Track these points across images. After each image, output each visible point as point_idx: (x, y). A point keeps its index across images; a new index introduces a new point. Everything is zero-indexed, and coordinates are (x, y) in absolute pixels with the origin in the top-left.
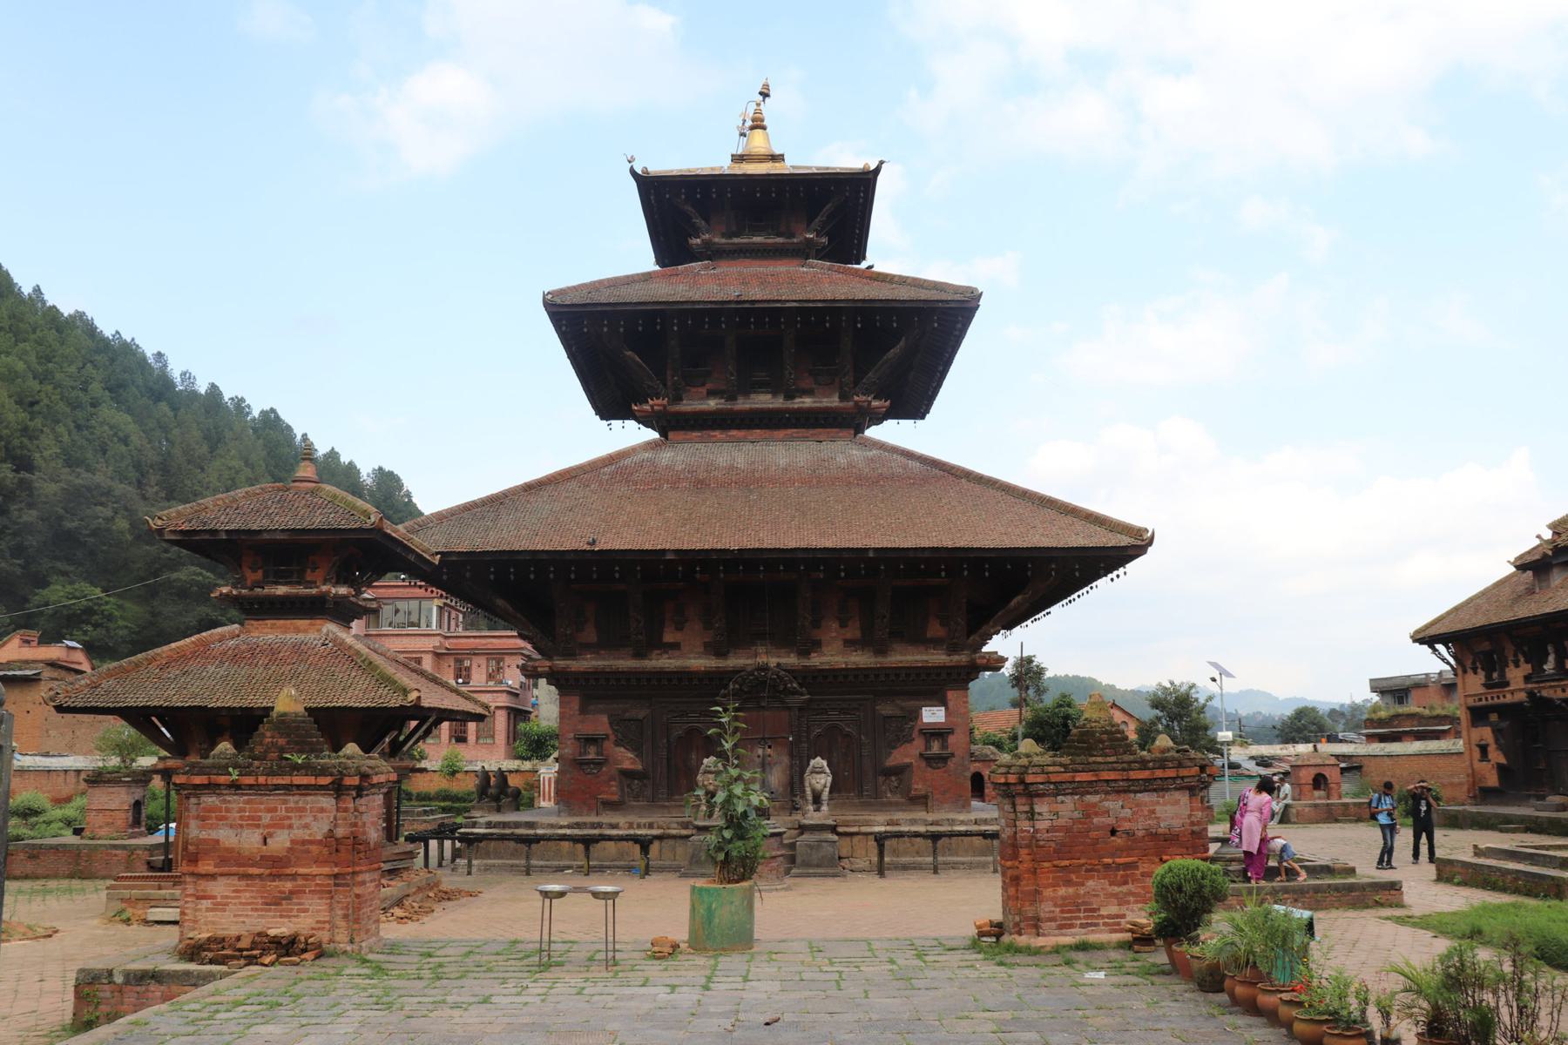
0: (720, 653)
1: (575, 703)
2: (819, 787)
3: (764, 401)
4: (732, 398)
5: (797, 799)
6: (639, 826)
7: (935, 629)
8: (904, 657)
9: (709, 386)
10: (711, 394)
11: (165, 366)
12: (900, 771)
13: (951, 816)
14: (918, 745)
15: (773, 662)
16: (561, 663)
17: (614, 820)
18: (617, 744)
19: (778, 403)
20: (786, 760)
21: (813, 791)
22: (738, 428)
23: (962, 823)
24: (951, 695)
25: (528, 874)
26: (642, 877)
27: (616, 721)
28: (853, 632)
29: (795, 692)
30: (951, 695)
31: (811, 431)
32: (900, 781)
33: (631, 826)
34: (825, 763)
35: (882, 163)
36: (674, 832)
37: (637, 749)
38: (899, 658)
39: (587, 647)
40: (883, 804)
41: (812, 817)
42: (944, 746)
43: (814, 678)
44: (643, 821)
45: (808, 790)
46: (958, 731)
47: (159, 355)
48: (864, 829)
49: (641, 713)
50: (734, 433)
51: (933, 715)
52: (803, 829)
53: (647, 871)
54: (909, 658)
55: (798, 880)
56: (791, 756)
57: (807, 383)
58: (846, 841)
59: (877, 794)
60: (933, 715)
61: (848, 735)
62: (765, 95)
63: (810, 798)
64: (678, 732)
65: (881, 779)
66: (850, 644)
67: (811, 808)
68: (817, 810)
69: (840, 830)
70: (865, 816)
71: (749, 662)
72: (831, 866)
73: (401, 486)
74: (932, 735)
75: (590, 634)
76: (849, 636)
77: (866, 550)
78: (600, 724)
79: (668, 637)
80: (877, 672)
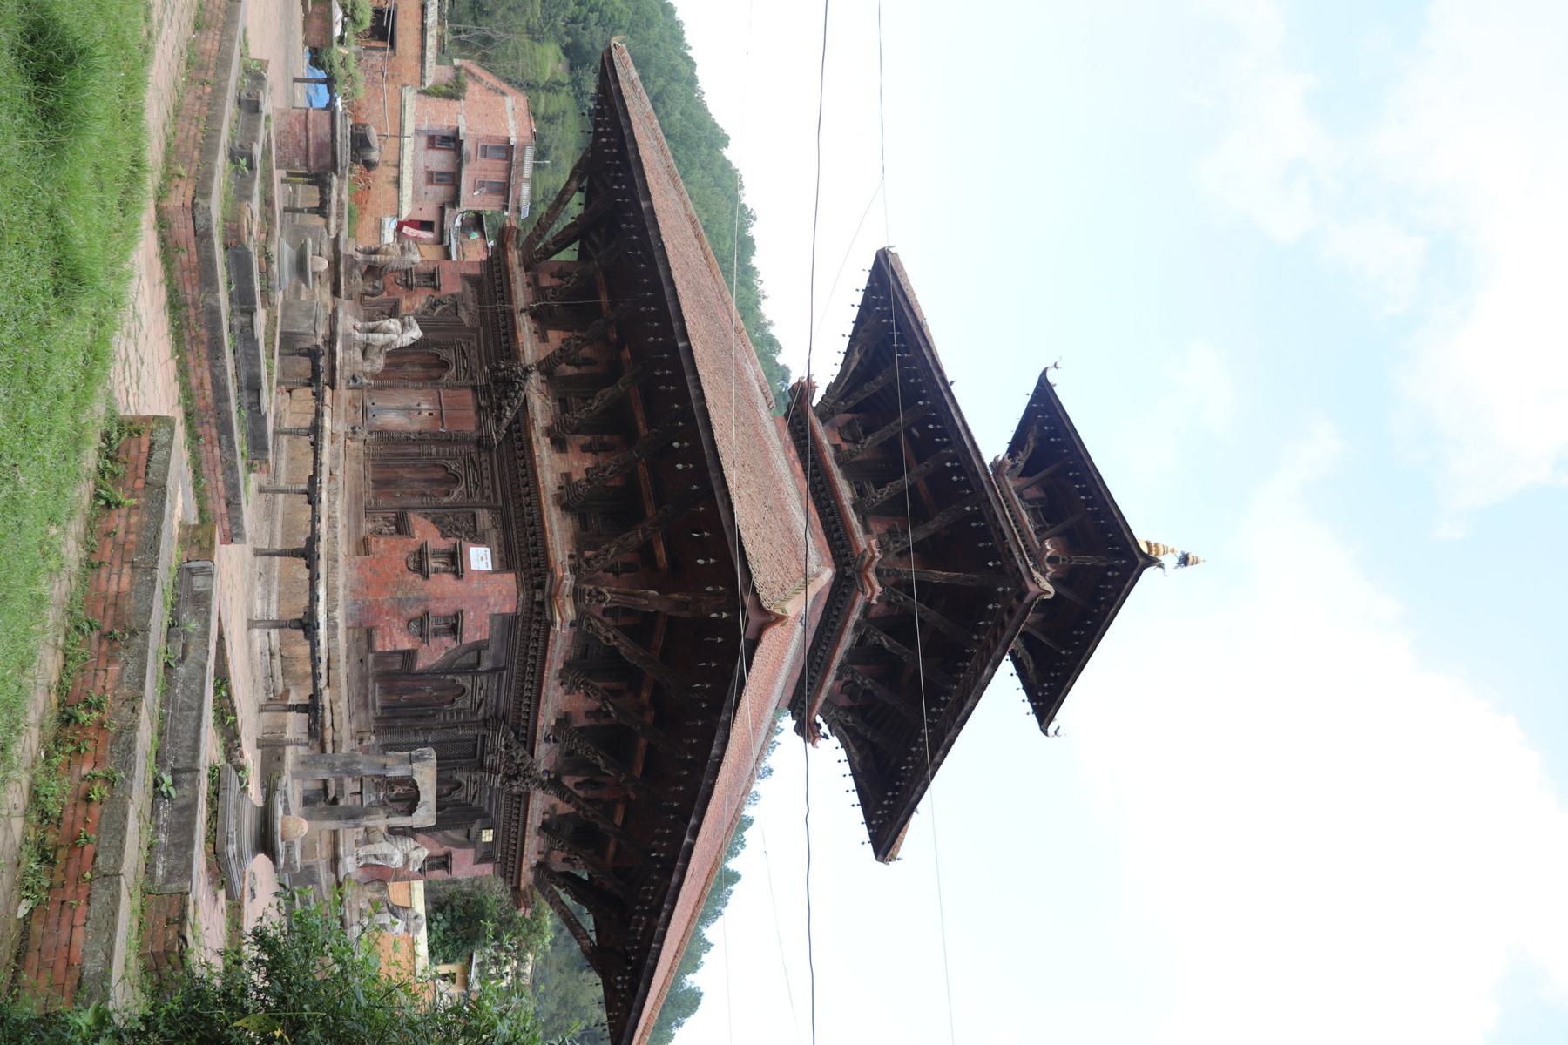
1: (476, 271)
3: (846, 492)
9: (845, 447)
10: (836, 447)
11: (760, 777)
12: (401, 527)
13: (341, 581)
20: (416, 427)
23: (332, 503)
24: (509, 579)
35: (1161, 566)
40: (358, 516)
42: (436, 571)
46: (460, 585)
47: (770, 771)
50: (799, 467)
51: (480, 558)
57: (878, 528)
59: (370, 511)
60: (480, 558)
62: (1185, 560)
73: (687, 1015)
77: (686, 337)
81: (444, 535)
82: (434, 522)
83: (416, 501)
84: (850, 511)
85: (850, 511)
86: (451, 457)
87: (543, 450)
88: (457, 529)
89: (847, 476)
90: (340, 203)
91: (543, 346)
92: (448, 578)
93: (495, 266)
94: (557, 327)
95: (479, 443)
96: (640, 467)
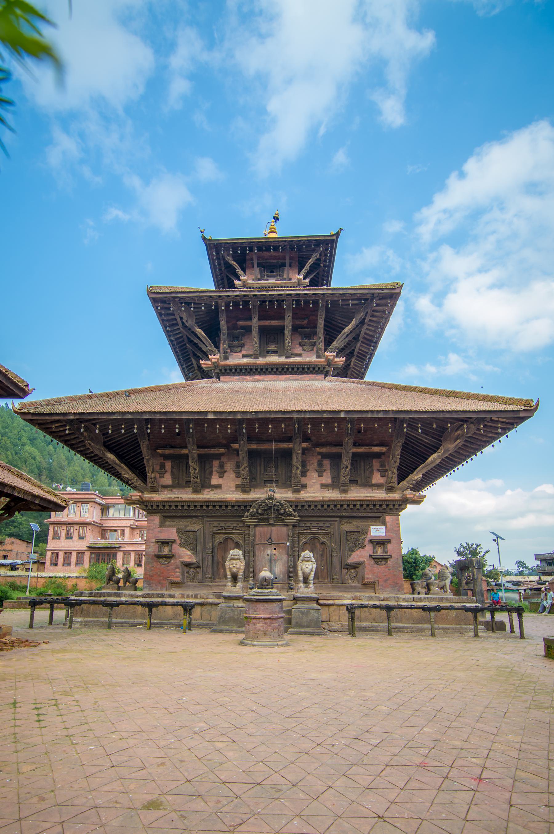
0: (244, 492)
1: (157, 520)
2: (307, 571)
4: (258, 358)
5: (292, 582)
6: (188, 597)
7: (377, 478)
8: (358, 494)
9: (244, 352)
12: (356, 566)
14: (368, 549)
15: (277, 496)
16: (147, 496)
17: (171, 592)
18: (181, 546)
19: (283, 360)
20: (285, 557)
21: (304, 573)
22: (260, 374)
24: (388, 519)
25: (109, 628)
26: (185, 632)
27: (181, 531)
28: (327, 479)
30: (388, 519)
31: (300, 376)
32: (357, 573)
33: (183, 596)
34: (311, 554)
36: (210, 601)
37: (193, 549)
38: (355, 495)
39: (165, 487)
40: (346, 588)
41: (303, 591)
43: (303, 506)
44: (190, 593)
45: (300, 574)
48: (337, 602)
49: (196, 527)
51: (377, 531)
52: (296, 600)
53: (190, 627)
54: (362, 495)
55: (294, 637)
56: (289, 555)
57: (298, 350)
58: (324, 610)
61: (323, 543)
63: (301, 578)
64: (220, 538)
65: (345, 571)
66: (324, 486)
67: (302, 585)
68: (307, 587)
69: (321, 602)
70: (335, 593)
71: (263, 496)
72: (316, 628)
74: (378, 543)
75: (168, 480)
76: (324, 482)
78: (171, 532)
80: (342, 503)
81: (364, 547)
82: (353, 551)
83: (336, 560)
84: (288, 360)
85: (288, 360)
86: (299, 542)
87: (304, 495)
88: (359, 541)
89: (264, 356)
90: (143, 596)
91: (224, 488)
92: (389, 547)
93: (150, 507)
94: (210, 479)
95: (294, 526)
96: (321, 451)
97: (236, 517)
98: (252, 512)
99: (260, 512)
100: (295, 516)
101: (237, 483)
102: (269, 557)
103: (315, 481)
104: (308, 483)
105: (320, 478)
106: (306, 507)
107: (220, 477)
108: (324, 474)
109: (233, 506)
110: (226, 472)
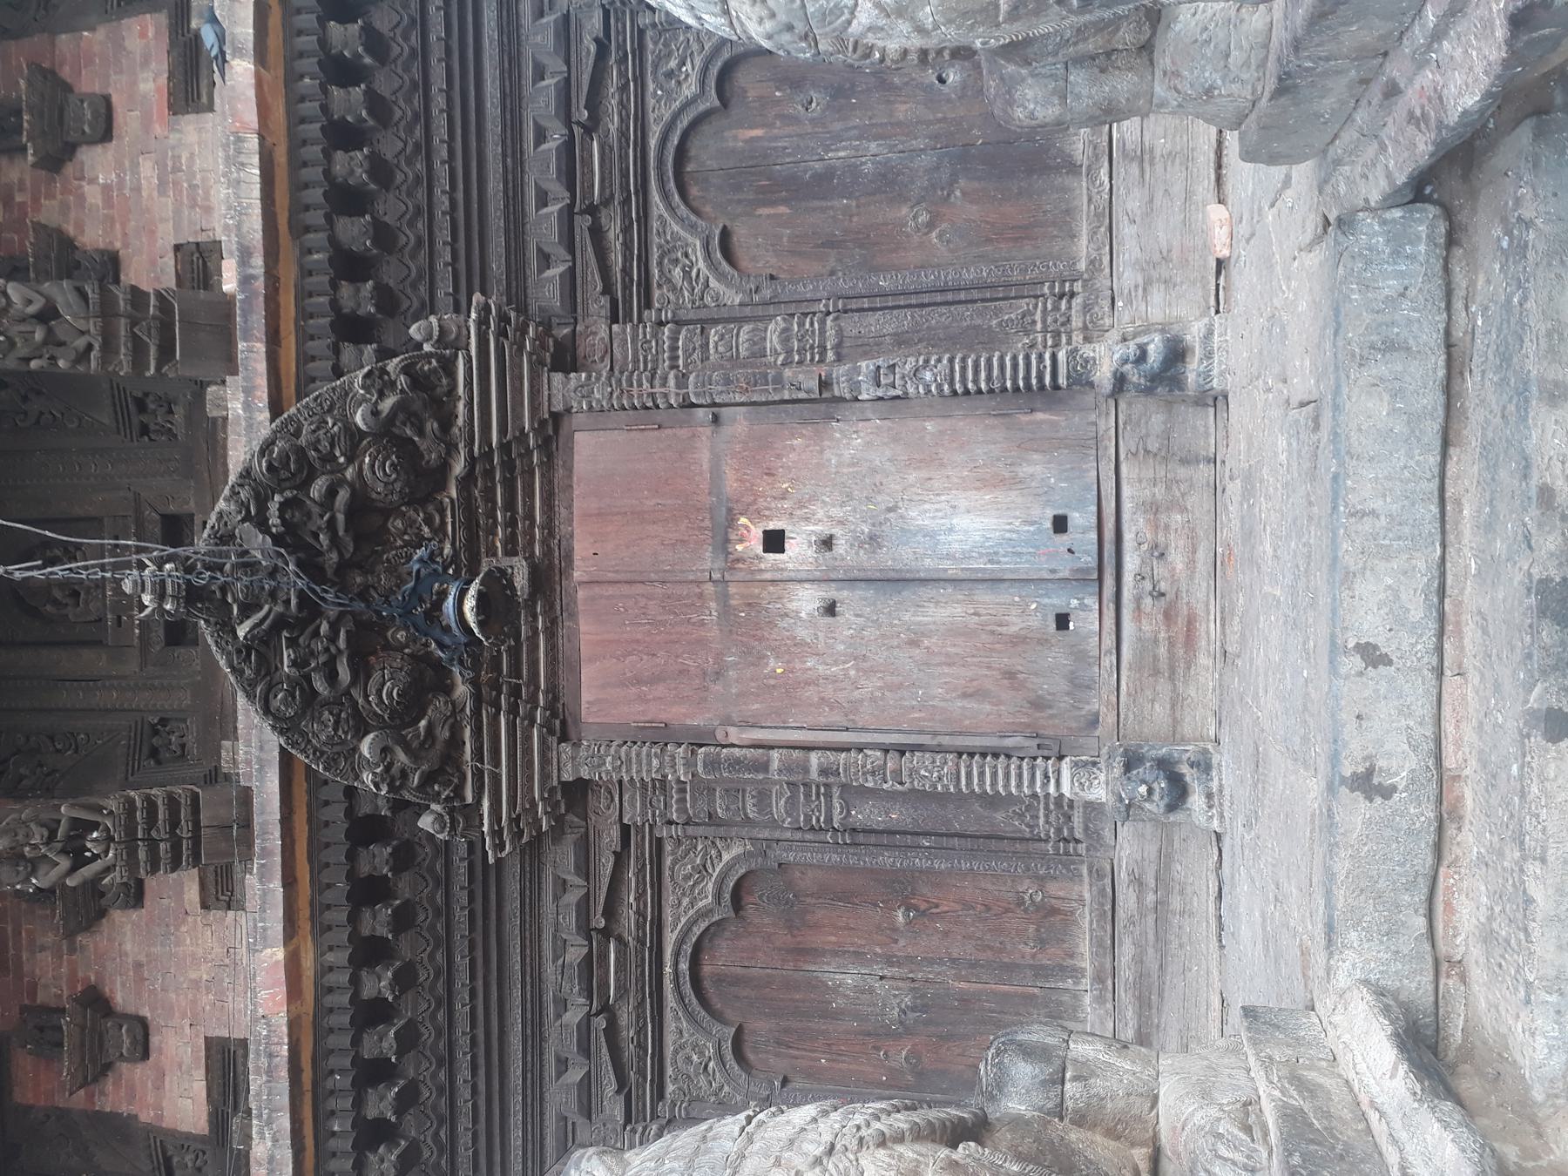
5: (1106, 358)
20: (854, 443)
29: (429, 391)
43: (350, 266)
56: (827, 402)
79: (182, 1103)
95: (566, 359)
97: (487, 914)
98: (396, 780)
99: (386, 687)
100: (449, 343)
101: (192, 893)
102: (842, 595)
103: (148, 170)
104: (167, 237)
105: (127, 121)
106: (354, 231)
107: (143, 1050)
108: (88, 84)
109: (369, 953)
110: (95, 1001)
